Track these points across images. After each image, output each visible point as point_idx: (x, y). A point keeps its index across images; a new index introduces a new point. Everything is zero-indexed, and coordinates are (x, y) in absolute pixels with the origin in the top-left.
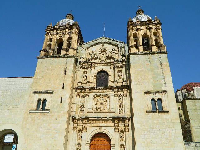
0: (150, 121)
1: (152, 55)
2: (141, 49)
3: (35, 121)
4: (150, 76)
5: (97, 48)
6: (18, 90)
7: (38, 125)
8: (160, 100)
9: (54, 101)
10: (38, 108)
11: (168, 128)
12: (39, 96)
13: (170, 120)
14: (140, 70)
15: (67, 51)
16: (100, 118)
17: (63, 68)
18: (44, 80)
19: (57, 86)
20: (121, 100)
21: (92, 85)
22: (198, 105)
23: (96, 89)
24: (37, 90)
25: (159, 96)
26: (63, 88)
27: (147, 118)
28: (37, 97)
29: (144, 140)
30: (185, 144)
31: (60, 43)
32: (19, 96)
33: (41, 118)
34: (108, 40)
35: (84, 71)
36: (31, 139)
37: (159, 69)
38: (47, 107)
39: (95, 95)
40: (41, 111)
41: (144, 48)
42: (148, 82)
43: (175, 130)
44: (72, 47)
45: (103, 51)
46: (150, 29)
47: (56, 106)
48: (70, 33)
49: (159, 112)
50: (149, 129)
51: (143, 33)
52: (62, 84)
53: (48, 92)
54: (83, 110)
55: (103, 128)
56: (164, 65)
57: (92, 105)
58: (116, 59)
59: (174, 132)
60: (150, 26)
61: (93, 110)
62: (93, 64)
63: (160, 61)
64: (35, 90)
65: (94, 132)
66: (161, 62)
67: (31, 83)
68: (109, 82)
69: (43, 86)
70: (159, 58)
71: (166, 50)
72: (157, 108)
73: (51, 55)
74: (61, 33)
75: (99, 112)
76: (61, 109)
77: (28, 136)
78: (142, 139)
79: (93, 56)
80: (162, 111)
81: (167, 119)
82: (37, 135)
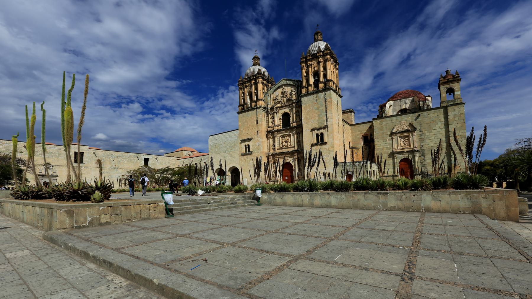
5: (279, 92)
13: (327, 149)
14: (309, 110)
17: (255, 119)
20: (299, 137)
22: (384, 123)
28: (244, 144)
35: (271, 116)
38: (251, 150)
39: (281, 135)
42: (314, 120)
44: (259, 98)
48: (256, 84)
54: (275, 148)
56: (328, 102)
61: (280, 147)
69: (245, 135)
72: (320, 141)
74: (249, 85)
79: (277, 101)
80: (323, 143)
81: (325, 149)
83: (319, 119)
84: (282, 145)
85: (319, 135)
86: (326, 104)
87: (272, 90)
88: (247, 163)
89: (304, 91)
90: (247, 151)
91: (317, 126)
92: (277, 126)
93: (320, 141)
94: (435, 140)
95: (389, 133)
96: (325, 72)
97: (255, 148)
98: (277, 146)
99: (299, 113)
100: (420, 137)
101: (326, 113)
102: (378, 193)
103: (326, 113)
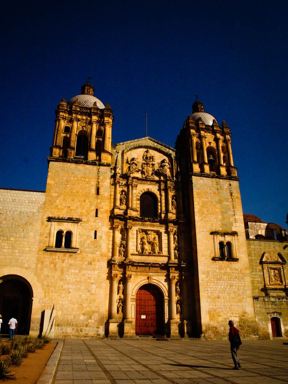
0: (217, 271)
1: (221, 180)
2: (207, 168)
3: (56, 264)
4: (218, 210)
6: (21, 212)
7: (62, 270)
8: (229, 244)
9: (84, 236)
11: (237, 280)
12: (59, 226)
13: (239, 270)
14: (205, 200)
15: (99, 154)
16: (150, 263)
17: (94, 183)
18: (64, 199)
19: (86, 211)
24: (53, 216)
25: (228, 238)
26: (97, 216)
27: (213, 267)
28: (55, 227)
29: (209, 294)
30: (253, 298)
32: (24, 223)
33: (66, 261)
34: (156, 144)
35: (121, 189)
36: (54, 291)
37: (228, 202)
38: (74, 244)
40: (66, 250)
41: (210, 167)
42: (215, 218)
43: (243, 282)
46: (216, 140)
47: (89, 245)
49: (227, 260)
50: (215, 282)
52: (93, 210)
53: (74, 221)
55: (154, 278)
59: (243, 285)
60: (218, 135)
62: (135, 180)
63: (231, 190)
64: (51, 216)
65: (141, 283)
66: (231, 192)
67: (41, 203)
68: (159, 211)
69: (63, 210)
70: (229, 185)
71: (237, 175)
73: (72, 157)
74: (83, 120)
75: (146, 255)
76: (96, 249)
77: (48, 286)
78: (208, 294)
80: (231, 258)
81: (236, 269)
82: (62, 286)
83: (223, 218)
84: (143, 249)
85: (225, 244)
86: (232, 199)
88: (58, 274)
89: (196, 168)
90: (63, 244)
91: (221, 230)
92: (132, 209)
96: (226, 155)
97: (88, 242)
98: (132, 247)
101: (234, 212)
103: (234, 212)
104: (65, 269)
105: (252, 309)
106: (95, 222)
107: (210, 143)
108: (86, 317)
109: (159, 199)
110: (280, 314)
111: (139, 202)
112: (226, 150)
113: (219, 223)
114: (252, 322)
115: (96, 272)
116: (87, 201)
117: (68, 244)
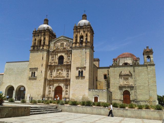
10: (32, 76)
17: (42, 56)
21: (56, 64)
23: (58, 66)
31: (40, 41)
35: (52, 56)
38: (35, 76)
44: (45, 44)
45: (62, 44)
46: (84, 32)
48: (44, 35)
51: (80, 34)
57: (55, 73)
58: (67, 50)
68: (64, 62)
85: (81, 71)
87: (55, 41)
90: (33, 76)
92: (55, 63)
93: (81, 75)
94: (142, 82)
95: (118, 75)
99: (70, 57)
100: (134, 79)
102: (123, 109)
104: (33, 83)
105: (88, 94)
106: (41, 68)
107: (81, 34)
108: (38, 96)
109: (64, 58)
110: (98, 96)
111: (58, 60)
112: (87, 35)
113: (80, 64)
114: (87, 98)
115: (41, 83)
116: (40, 62)
117: (34, 76)
